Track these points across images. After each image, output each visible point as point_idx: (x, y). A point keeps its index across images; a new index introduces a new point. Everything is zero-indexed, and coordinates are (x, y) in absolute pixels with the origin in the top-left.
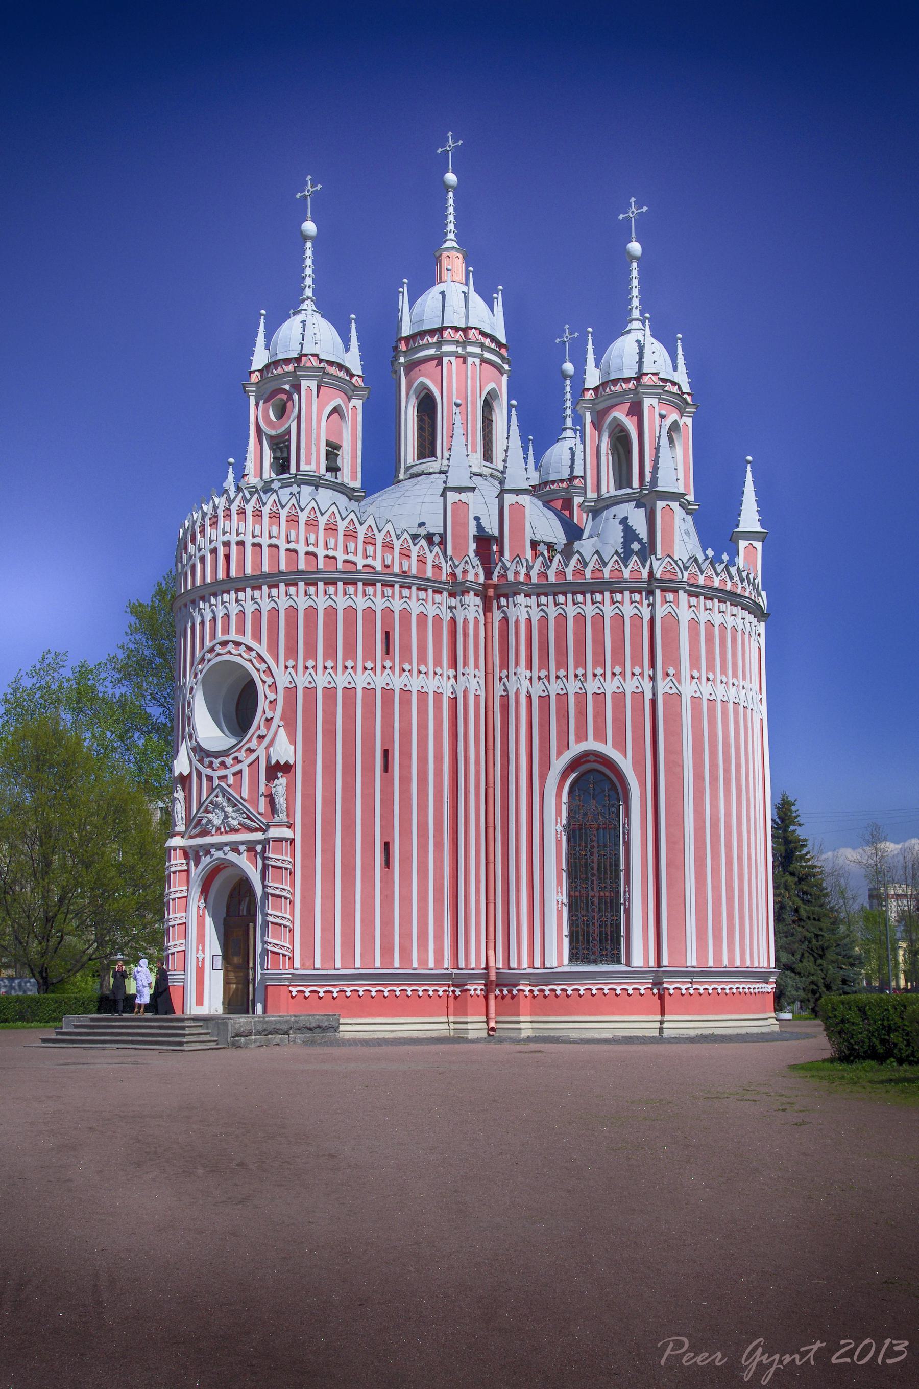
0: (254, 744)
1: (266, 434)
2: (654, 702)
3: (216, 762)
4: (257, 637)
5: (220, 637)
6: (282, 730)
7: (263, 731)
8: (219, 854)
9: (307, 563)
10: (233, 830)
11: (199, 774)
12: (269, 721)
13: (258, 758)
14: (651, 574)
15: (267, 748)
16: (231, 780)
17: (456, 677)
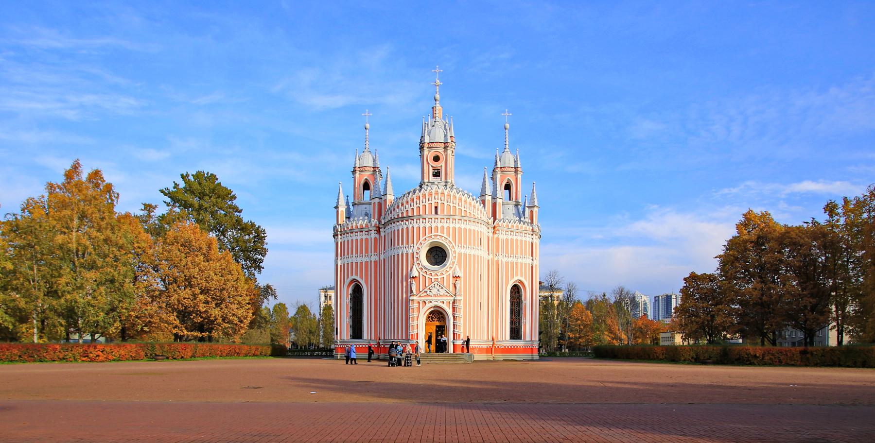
2: (532, 266)
5: (433, 233)
9: (464, 213)
12: (453, 263)
14: (533, 230)
16: (439, 280)
17: (489, 254)
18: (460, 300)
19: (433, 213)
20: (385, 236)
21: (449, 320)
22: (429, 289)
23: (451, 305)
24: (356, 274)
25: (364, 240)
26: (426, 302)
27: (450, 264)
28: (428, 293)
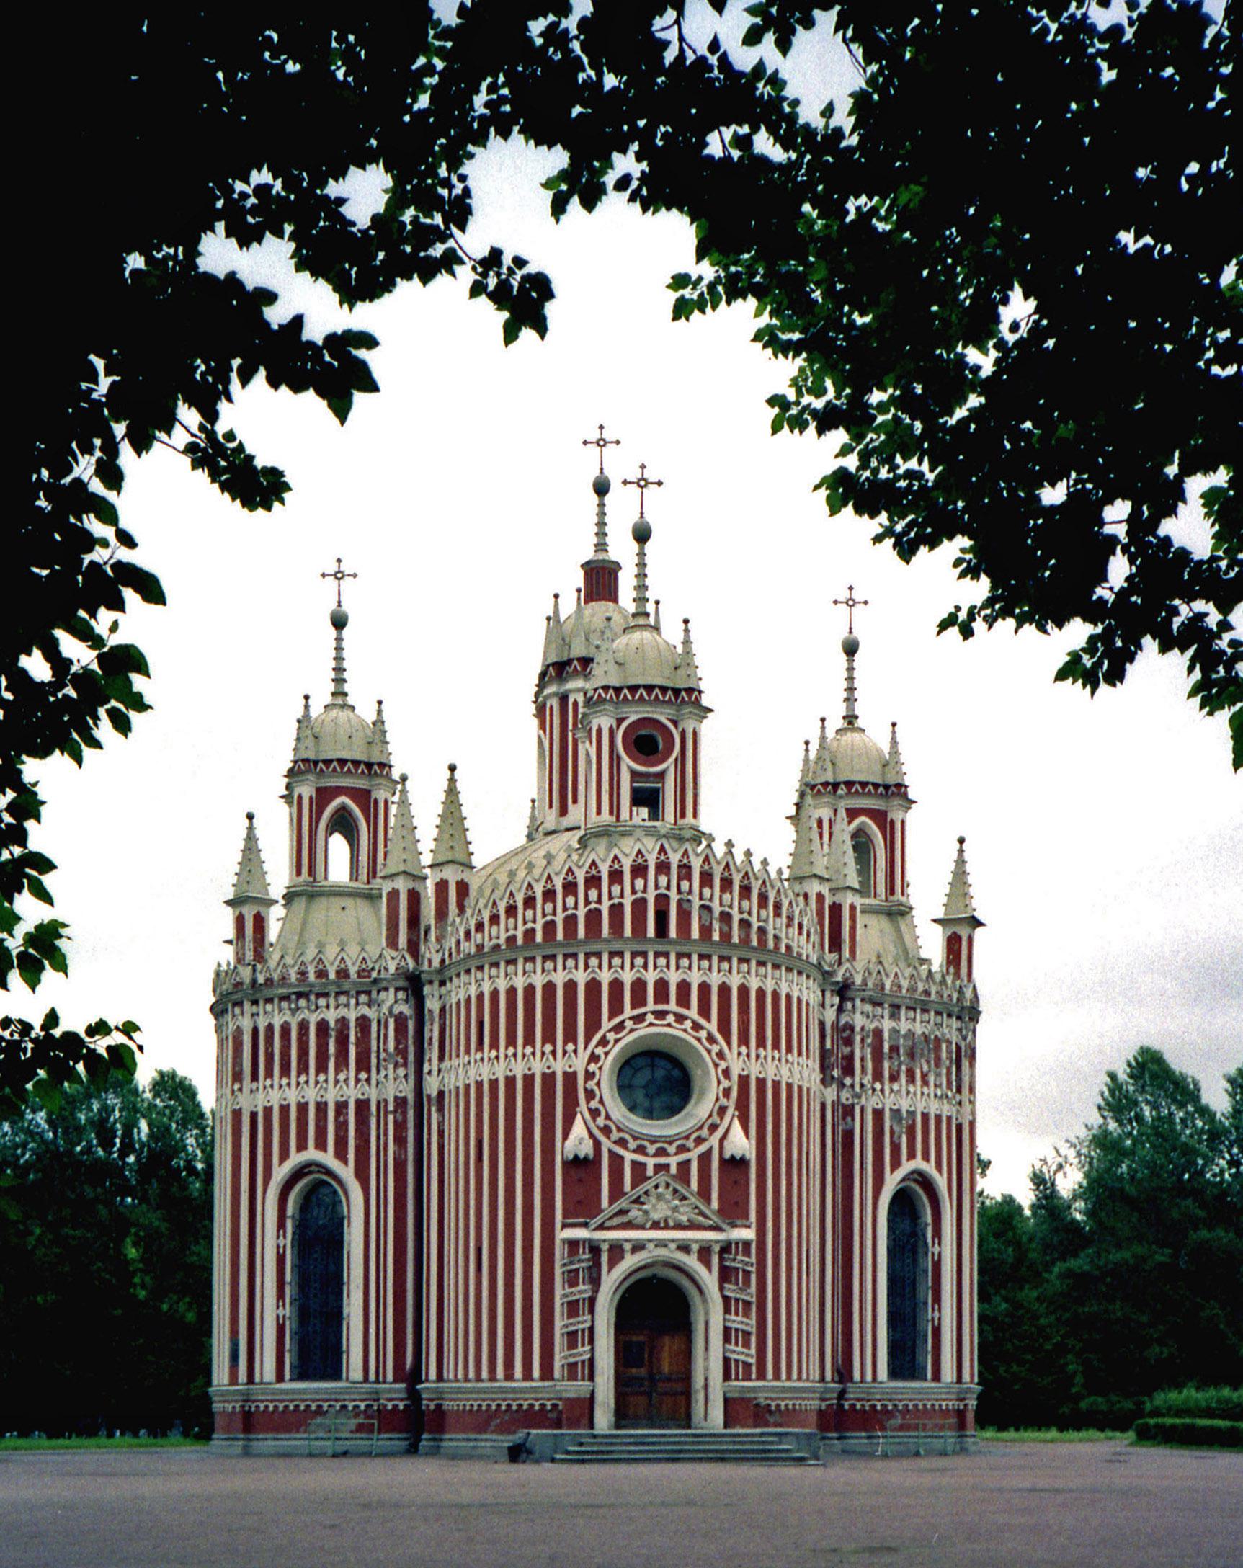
0: (705, 1133)
1: (629, 767)
3: (651, 1149)
4: (704, 1011)
5: (651, 1006)
6: (736, 1122)
7: (716, 1119)
8: (662, 1252)
10: (679, 1227)
11: (616, 1160)
12: (722, 1111)
13: (710, 1151)
15: (722, 1140)
18: (747, 1244)
19: (651, 932)
20: (443, 1010)
21: (707, 1313)
22: (637, 1201)
23: (715, 1260)
24: (321, 1145)
25: (352, 1024)
26: (627, 1246)
27: (710, 1116)
28: (635, 1213)
